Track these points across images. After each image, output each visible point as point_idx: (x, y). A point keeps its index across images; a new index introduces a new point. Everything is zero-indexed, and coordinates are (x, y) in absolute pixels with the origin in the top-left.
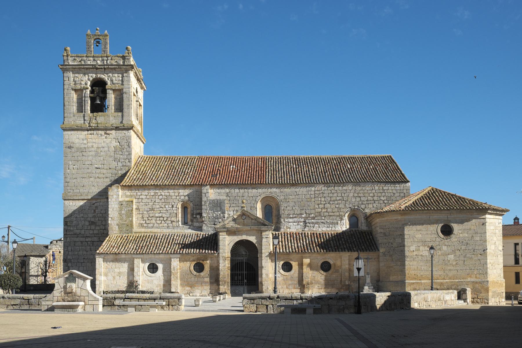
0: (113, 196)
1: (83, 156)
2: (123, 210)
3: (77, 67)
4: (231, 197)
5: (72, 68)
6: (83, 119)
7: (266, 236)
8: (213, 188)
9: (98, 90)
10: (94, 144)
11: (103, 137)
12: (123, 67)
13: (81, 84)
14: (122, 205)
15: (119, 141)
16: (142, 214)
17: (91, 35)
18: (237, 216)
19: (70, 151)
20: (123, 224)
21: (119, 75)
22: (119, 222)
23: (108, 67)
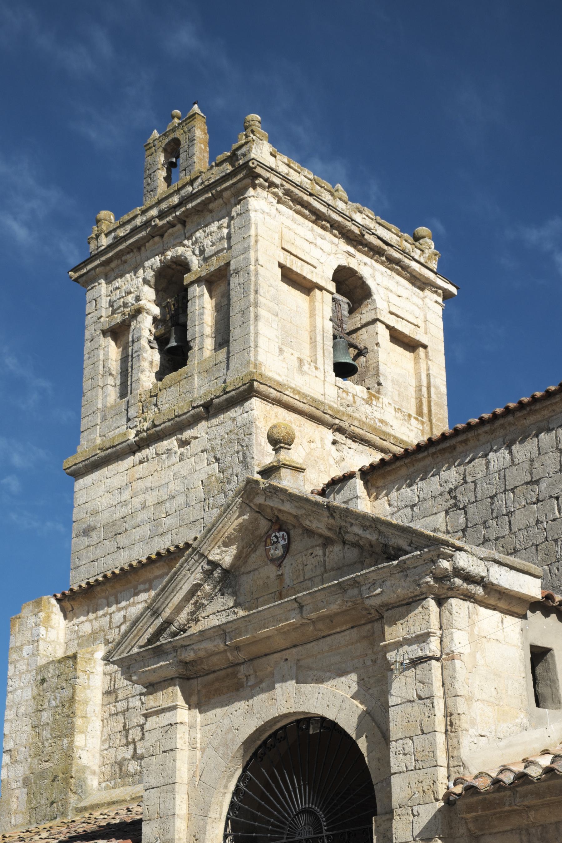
0: (20, 649)
1: (118, 548)
2: (46, 706)
3: (111, 254)
4: (471, 509)
5: (102, 264)
6: (125, 419)
7: (415, 651)
8: (384, 487)
9: (174, 305)
10: (147, 497)
11: (174, 459)
12: (224, 186)
13: (125, 305)
14: (43, 681)
15: (218, 456)
16: (123, 712)
17: (156, 142)
18: (233, 550)
19: (87, 543)
20: (42, 775)
21: (221, 222)
22: (30, 768)
23: (183, 209)
